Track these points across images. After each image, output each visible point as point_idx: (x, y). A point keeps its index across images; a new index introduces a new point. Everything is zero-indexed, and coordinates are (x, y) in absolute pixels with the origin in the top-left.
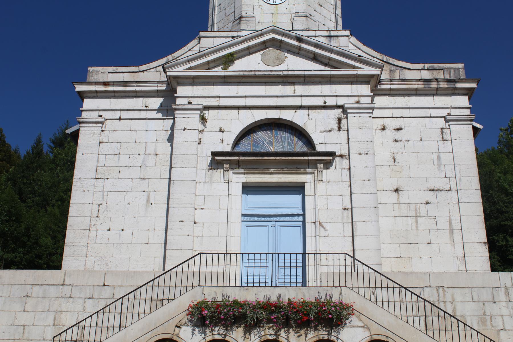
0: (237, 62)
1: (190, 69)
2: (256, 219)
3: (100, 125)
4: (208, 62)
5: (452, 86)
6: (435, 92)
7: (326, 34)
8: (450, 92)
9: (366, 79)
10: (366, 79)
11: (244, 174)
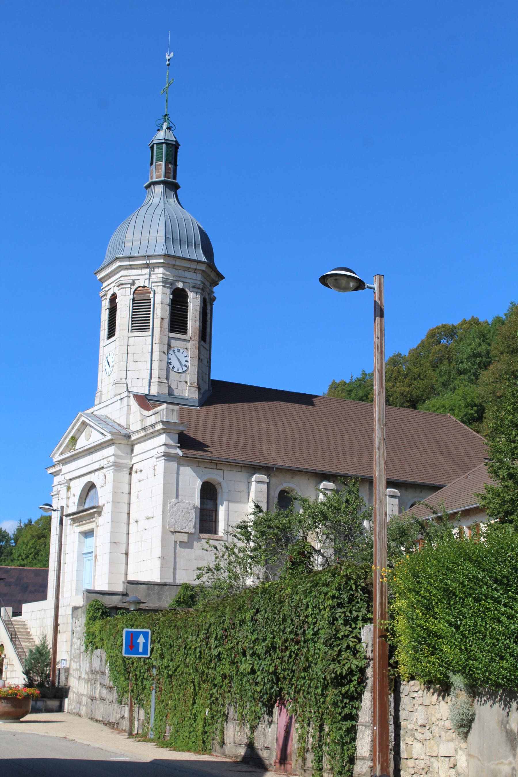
0: (78, 441)
1: (62, 454)
2: (87, 555)
3: (57, 496)
4: (67, 446)
6: (152, 435)
7: (119, 397)
8: (157, 433)
9: (112, 442)
10: (112, 442)
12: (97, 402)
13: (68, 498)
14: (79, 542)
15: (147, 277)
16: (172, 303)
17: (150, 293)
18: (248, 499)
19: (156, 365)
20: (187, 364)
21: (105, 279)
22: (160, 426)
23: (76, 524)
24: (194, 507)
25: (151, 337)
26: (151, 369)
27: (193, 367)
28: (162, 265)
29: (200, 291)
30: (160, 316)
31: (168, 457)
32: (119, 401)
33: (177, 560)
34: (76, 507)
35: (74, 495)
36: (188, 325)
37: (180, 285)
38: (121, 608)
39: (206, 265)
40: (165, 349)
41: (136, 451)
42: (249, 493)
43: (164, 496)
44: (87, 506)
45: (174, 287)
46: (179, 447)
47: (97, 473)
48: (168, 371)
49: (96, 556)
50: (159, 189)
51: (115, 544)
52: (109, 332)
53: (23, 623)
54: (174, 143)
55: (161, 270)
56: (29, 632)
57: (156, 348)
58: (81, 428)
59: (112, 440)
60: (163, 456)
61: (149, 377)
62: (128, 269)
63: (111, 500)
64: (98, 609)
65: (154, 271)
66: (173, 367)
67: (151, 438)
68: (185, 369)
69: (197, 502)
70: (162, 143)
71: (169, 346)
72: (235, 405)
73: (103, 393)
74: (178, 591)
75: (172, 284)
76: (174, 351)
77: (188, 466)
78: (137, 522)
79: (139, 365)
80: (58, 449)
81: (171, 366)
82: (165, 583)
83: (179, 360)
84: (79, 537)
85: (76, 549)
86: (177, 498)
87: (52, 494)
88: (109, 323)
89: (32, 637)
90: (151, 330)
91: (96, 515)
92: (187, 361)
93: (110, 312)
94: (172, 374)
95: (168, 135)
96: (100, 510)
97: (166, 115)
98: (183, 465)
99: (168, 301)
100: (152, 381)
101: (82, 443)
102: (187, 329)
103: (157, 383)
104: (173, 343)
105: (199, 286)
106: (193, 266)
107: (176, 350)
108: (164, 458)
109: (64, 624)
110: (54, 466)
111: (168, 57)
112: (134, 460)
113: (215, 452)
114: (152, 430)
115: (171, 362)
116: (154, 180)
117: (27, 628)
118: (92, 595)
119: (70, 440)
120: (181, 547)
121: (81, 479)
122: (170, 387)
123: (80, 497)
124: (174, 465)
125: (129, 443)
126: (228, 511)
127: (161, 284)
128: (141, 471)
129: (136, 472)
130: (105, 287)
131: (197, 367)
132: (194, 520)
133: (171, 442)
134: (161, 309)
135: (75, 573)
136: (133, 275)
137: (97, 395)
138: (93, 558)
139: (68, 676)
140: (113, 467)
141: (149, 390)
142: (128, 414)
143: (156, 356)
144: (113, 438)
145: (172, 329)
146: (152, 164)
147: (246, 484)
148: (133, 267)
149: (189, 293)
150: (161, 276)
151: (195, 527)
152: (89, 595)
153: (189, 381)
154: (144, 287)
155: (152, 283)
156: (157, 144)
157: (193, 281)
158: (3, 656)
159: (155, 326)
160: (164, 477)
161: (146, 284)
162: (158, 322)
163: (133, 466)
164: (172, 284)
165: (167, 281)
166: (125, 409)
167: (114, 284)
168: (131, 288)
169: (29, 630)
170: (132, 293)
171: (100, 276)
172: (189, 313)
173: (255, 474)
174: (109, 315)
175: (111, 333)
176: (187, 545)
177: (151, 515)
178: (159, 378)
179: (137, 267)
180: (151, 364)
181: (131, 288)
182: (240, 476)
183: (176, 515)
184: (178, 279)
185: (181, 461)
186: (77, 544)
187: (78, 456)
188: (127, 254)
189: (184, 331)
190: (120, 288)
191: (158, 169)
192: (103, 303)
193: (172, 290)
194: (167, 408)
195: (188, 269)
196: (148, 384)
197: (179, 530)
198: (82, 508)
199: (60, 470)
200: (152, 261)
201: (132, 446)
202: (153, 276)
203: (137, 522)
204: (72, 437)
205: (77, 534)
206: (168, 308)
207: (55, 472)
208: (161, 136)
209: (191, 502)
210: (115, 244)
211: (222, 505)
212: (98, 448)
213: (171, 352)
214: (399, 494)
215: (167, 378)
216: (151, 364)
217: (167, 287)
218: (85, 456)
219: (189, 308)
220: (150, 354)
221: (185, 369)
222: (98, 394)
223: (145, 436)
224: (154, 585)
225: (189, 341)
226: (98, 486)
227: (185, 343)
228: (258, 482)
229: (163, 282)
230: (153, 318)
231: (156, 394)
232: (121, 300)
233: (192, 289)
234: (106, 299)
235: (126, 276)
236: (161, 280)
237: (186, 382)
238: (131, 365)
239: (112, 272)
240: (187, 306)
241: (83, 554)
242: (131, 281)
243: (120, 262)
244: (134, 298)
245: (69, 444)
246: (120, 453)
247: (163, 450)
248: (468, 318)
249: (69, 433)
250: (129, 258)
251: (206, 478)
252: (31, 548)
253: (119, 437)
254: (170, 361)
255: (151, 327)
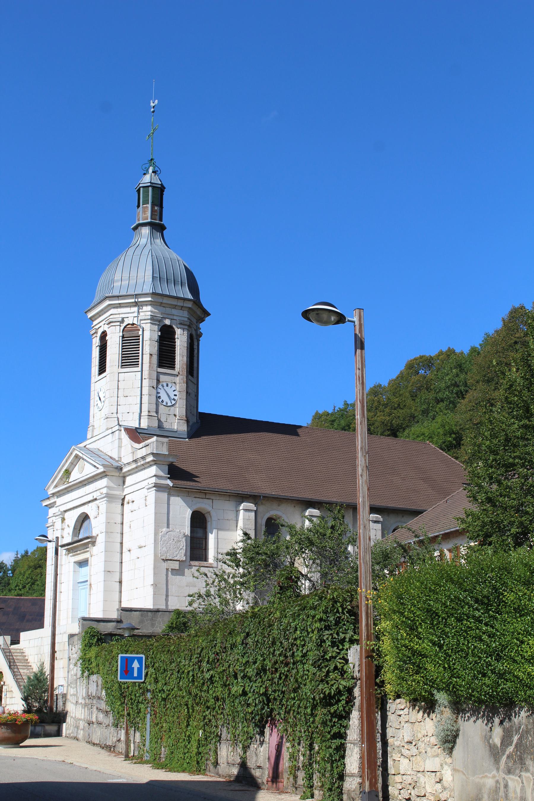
1: (56, 486)
2: (82, 584)
3: (52, 527)
4: (61, 479)
5: (144, 462)
6: (143, 467)
7: (110, 431)
8: (148, 465)
9: (104, 474)
10: (104, 474)
11: (74, 555)
12: (89, 436)
13: (63, 529)
14: (74, 571)
15: (136, 314)
16: (160, 340)
17: (139, 330)
18: (237, 526)
19: (145, 399)
20: (176, 398)
21: (96, 317)
22: (150, 458)
23: (71, 554)
24: (186, 536)
25: (140, 373)
26: (141, 403)
27: (182, 401)
28: (150, 303)
29: (186, 327)
30: (148, 352)
31: (158, 487)
32: (111, 435)
33: (170, 587)
34: (71, 537)
35: (68, 526)
36: (176, 360)
37: (167, 322)
38: (115, 635)
39: (192, 303)
40: (154, 384)
41: (127, 483)
42: (237, 521)
43: (155, 526)
44: (81, 537)
45: (162, 324)
46: (169, 478)
47: (90, 504)
48: (157, 405)
49: (91, 585)
50: (146, 231)
51: (109, 573)
52: (99, 368)
53: (22, 651)
54: (160, 186)
55: (149, 308)
56: (27, 660)
57: (146, 383)
58: (74, 462)
59: (104, 472)
60: (154, 487)
61: (139, 411)
62: (117, 307)
63: (104, 531)
64: (94, 636)
65: (142, 309)
66: (162, 401)
67: (142, 470)
68: (173, 402)
69: (187, 531)
70: (148, 186)
71: (158, 381)
72: (223, 436)
73: (95, 427)
74: (171, 617)
75: (159, 321)
76: (163, 386)
77: (178, 496)
78: (129, 551)
79: (130, 400)
80: (53, 482)
81: (160, 400)
82: (158, 609)
83: (168, 394)
84: (74, 566)
85: (71, 578)
86: (168, 527)
87: (47, 526)
88: (100, 360)
89: (30, 664)
90: (140, 365)
91: (90, 545)
92: (175, 395)
93: (100, 349)
94: (161, 407)
95: (154, 179)
96: (94, 540)
97: (152, 159)
98: (174, 495)
99: (156, 338)
100: (142, 415)
101: (76, 476)
102: (175, 365)
103: (147, 417)
104: (162, 378)
105: (185, 323)
106: (180, 303)
107: (165, 385)
108: (154, 488)
109: (61, 651)
110: (48, 498)
111: (152, 104)
112: (126, 491)
113: (204, 483)
114: (142, 462)
115: (160, 397)
116: (141, 222)
117: (25, 656)
118: (88, 622)
119: (64, 473)
120: (172, 574)
121: (75, 510)
122: (159, 421)
123: (74, 528)
124: (165, 495)
125: (121, 475)
126: (217, 539)
127: (149, 321)
128: (133, 502)
129: (128, 503)
130: (95, 325)
131: (185, 401)
132: (185, 548)
133: (161, 473)
134: (150, 345)
135: (71, 601)
136: (122, 313)
137: (89, 429)
138: (88, 586)
139: (65, 701)
140: (105, 499)
141: (140, 424)
142: (120, 447)
143: (146, 391)
144: (105, 470)
145: (161, 364)
146: (138, 206)
147: (235, 512)
148: (122, 305)
149: (176, 329)
150: (149, 313)
151: (185, 555)
152: (85, 622)
153: (177, 414)
154: (133, 324)
155: (141, 320)
156: (143, 187)
157: (180, 318)
158: (2, 683)
159: (144, 362)
160: (155, 507)
161: (135, 322)
162: (146, 358)
163: (125, 497)
164: (159, 321)
165: (155, 318)
166: (117, 442)
167: (104, 322)
168: (120, 326)
169: (27, 658)
170: (121, 331)
171: (90, 315)
172: (176, 349)
173: (242, 502)
174: (100, 352)
175: (102, 369)
176: (179, 572)
177: (143, 545)
178: (149, 411)
179: (126, 305)
180: (141, 398)
181: (120, 326)
182: (229, 505)
183: (167, 543)
184: (165, 316)
185: (171, 491)
186: (72, 573)
187: (72, 488)
188: (116, 293)
189: (172, 366)
190: (110, 325)
191: (144, 212)
192: (94, 340)
193: (160, 327)
194: (157, 441)
195: (175, 307)
196: (138, 417)
197: (170, 558)
198: (76, 539)
199: (55, 502)
200: (140, 300)
201: (124, 477)
202: (141, 314)
203: (129, 551)
204: (66, 470)
205: (72, 564)
206: (156, 344)
207: (50, 504)
208: (147, 179)
209: (182, 531)
210: (105, 284)
211: (212, 533)
212: (91, 480)
213: (160, 386)
214: (381, 520)
215: (157, 412)
216: (141, 398)
217: (155, 324)
218: (79, 488)
219: (176, 344)
220: (140, 389)
221: (173, 402)
222: (90, 429)
223: (136, 468)
224: (147, 611)
225: (178, 375)
226: (91, 516)
227: (173, 378)
228: (246, 510)
229: (151, 319)
230: (143, 354)
231: (146, 428)
232: (111, 338)
233: (179, 326)
234: (96, 336)
235: (116, 314)
236: (149, 317)
237: (175, 415)
238: (122, 400)
239: (102, 310)
240: (175, 342)
241: (78, 583)
242: (120, 319)
243: (110, 300)
244: (123, 335)
245: (63, 477)
246: (112, 485)
247: (154, 482)
248: (445, 349)
249: (63, 466)
250: (118, 297)
251: (195, 508)
252: (28, 578)
253: (111, 469)
254: (159, 395)
255: (140, 363)
